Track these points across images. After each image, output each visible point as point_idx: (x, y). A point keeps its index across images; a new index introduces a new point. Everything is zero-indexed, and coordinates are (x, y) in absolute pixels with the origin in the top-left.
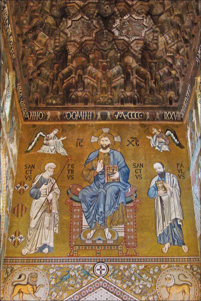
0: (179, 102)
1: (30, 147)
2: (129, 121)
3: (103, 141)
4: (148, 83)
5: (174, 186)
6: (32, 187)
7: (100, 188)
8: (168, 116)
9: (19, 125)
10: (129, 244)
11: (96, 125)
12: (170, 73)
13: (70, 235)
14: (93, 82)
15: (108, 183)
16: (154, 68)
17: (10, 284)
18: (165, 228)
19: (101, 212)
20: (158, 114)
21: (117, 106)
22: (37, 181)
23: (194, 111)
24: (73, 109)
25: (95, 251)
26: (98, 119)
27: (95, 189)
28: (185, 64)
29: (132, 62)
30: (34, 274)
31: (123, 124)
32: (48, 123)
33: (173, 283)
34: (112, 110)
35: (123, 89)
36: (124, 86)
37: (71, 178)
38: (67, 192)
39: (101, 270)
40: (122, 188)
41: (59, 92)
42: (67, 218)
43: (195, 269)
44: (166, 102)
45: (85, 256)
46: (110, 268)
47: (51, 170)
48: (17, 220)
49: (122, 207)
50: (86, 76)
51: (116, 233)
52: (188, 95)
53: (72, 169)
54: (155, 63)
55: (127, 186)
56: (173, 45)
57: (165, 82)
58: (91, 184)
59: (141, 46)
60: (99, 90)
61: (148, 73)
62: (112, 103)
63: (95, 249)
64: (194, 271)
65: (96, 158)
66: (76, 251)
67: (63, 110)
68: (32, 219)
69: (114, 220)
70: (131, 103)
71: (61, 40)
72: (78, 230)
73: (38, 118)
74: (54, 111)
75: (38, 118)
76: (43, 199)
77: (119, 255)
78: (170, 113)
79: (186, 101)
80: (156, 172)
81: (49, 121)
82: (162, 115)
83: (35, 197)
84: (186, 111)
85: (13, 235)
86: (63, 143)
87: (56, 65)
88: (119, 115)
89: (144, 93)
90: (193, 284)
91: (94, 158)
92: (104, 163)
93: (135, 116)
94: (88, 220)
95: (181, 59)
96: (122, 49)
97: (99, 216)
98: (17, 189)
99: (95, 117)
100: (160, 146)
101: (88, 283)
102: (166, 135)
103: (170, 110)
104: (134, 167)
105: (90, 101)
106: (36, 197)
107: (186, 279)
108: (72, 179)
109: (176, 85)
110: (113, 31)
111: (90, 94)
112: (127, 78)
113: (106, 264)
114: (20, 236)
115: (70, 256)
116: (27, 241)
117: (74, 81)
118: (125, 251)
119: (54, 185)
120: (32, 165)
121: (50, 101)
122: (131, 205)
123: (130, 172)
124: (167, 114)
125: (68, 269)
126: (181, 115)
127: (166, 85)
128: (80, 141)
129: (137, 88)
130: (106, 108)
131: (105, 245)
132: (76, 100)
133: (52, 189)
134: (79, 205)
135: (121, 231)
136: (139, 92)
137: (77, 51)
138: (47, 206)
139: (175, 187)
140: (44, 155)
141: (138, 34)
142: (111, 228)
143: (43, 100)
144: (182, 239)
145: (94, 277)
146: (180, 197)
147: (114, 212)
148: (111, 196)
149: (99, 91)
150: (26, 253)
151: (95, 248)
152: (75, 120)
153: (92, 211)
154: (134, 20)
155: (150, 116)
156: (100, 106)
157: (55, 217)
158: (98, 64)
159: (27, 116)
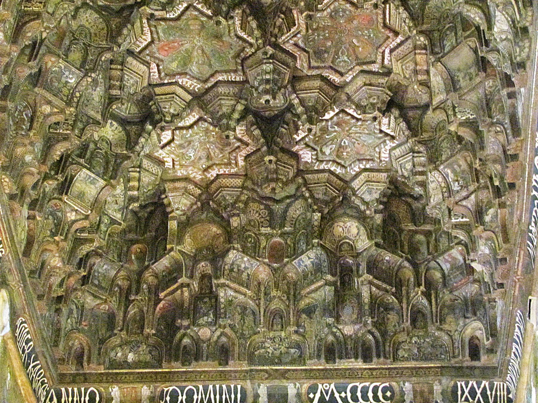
0: (498, 353)
16: (423, 249)
20: (437, 388)
21: (314, 367)
24: (188, 377)
29: (358, 234)
34: (300, 379)
41: (146, 326)
44: (459, 355)
50: (222, 281)
54: (428, 234)
56: (466, 198)
57: (456, 293)
59: (382, 188)
60: (262, 318)
61: (406, 264)
62: (301, 359)
70: (356, 358)
71: (146, 179)
74: (131, 385)
78: (475, 386)
82: (449, 390)
87: (136, 248)
88: (321, 392)
89: (395, 326)
96: (326, 198)
105: (236, 356)
110: (294, 149)
111: (236, 333)
117: (186, 294)
124: (467, 387)
126: (509, 392)
127: (459, 301)
129: (372, 314)
130: (284, 375)
136: (380, 325)
137: (195, 207)
141: (370, 156)
143: (97, 352)
149: (262, 321)
154: (354, 121)
155: (414, 394)
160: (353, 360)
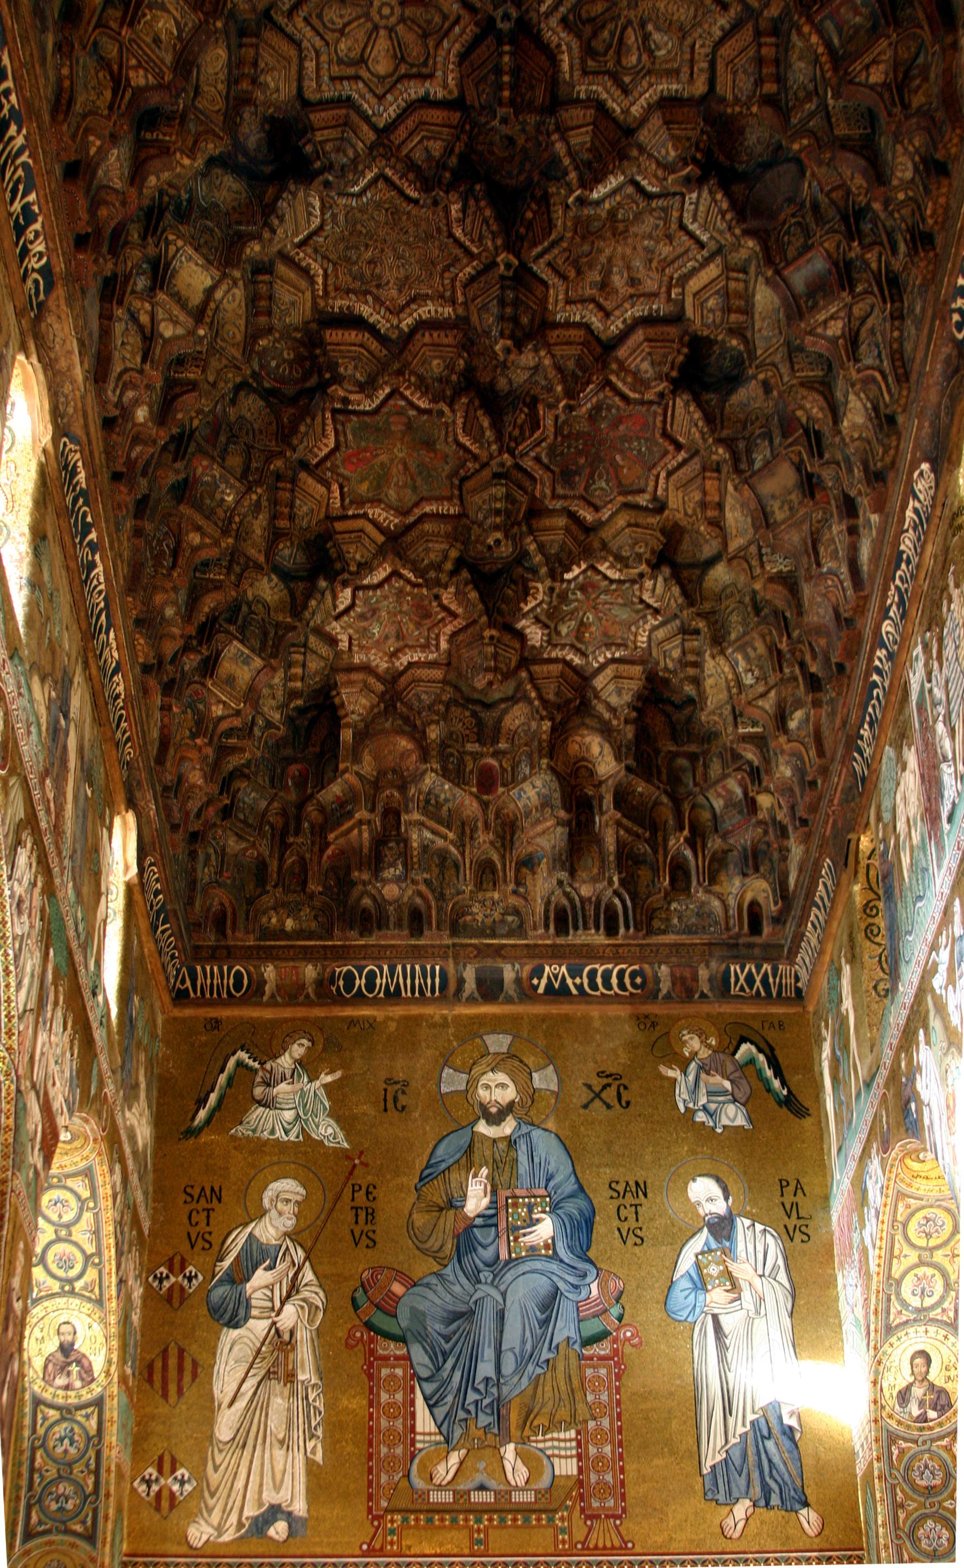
1: (202, 1114)
2: (590, 1003)
3: (488, 1087)
4: (666, 841)
6: (214, 1276)
7: (479, 1282)
8: (746, 979)
9: (154, 1021)
11: (457, 1018)
12: (752, 805)
13: (370, 1471)
14: (445, 841)
15: (510, 1260)
18: (733, 1441)
19: (487, 1380)
20: (703, 973)
23: (847, 969)
25: (465, 1532)
26: (465, 995)
27: (460, 1285)
28: (808, 778)
31: (566, 1015)
32: (268, 1014)
35: (563, 869)
38: (354, 1300)
42: (356, 1403)
45: (427, 1552)
47: (289, 1209)
48: (163, 1409)
49: (567, 1358)
51: (545, 1461)
53: (368, 1204)
62: (520, 931)
63: (467, 1527)
66: (392, 1532)
67: (325, 959)
72: (399, 1451)
76: (258, 1327)
77: (556, 1546)
80: (698, 1215)
83: (227, 1316)
84: (816, 962)
85: (150, 1470)
86: (329, 1098)
91: (451, 1161)
92: (491, 1178)
93: (614, 981)
94: (436, 1410)
95: (793, 754)
97: (477, 1397)
98: (156, 1284)
99: (452, 987)
100: (712, 1106)
102: (735, 1062)
103: (750, 958)
109: (776, 855)
112: (579, 824)
114: (178, 1473)
115: (370, 1552)
116: (206, 1494)
118: (579, 1535)
120: (212, 1189)
126: (797, 979)
130: (498, 951)
134: (402, 1352)
139: (774, 1276)
142: (524, 1441)
144: (799, 1483)
146: (791, 1315)
147: (536, 1382)
150: (205, 1538)
151: (466, 1520)
152: (375, 1001)
153: (451, 1376)
158: (461, 763)
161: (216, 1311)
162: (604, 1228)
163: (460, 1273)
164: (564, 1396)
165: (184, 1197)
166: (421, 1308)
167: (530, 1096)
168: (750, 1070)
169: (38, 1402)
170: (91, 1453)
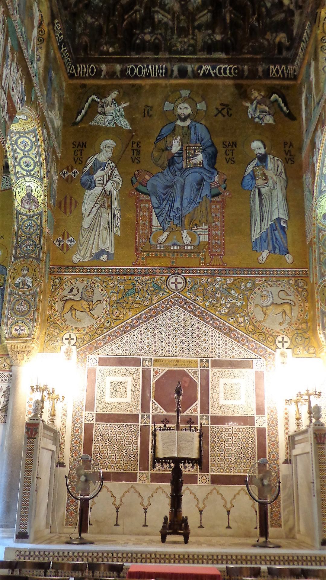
1: (79, 117)
3: (181, 108)
5: (278, 174)
7: (176, 175)
9: (61, 85)
10: (214, 251)
11: (171, 85)
13: (136, 238)
15: (187, 168)
17: (59, 299)
18: (264, 231)
20: (260, 69)
22: (90, 165)
23: (313, 63)
27: (169, 176)
30: (89, 288)
32: (103, 82)
33: (270, 302)
36: (211, 26)
37: (136, 161)
38: (132, 181)
39: (176, 283)
40: (206, 176)
42: (131, 215)
43: (300, 285)
46: (188, 281)
49: (206, 202)
50: (157, 9)
52: (305, 38)
53: (138, 148)
55: (213, 174)
57: (273, 19)
58: (164, 170)
62: (194, 53)
64: (299, 287)
65: (172, 134)
66: (143, 259)
68: (84, 216)
69: (194, 219)
70: (222, 52)
72: (146, 232)
73: (89, 74)
75: (89, 74)
76: (98, 190)
77: (200, 264)
78: (279, 68)
79: (303, 49)
81: (105, 78)
84: (302, 63)
85: (60, 237)
90: (296, 303)
91: (167, 134)
92: (181, 140)
93: (228, 71)
94: (159, 218)
100: (261, 116)
101: (159, 300)
104: (224, 147)
106: (89, 187)
107: (288, 298)
108: (138, 162)
113: (183, 276)
114: (70, 239)
116: (79, 246)
117: (138, 16)
118: (208, 260)
119: (113, 170)
120: (83, 143)
121: (105, 48)
122: (218, 199)
123: (218, 154)
125: (133, 281)
128: (148, 108)
130: (186, 60)
131: (182, 251)
132: (143, 47)
133: (111, 176)
135: (203, 233)
138: (104, 199)
139: (280, 175)
140: (99, 128)
142: (190, 229)
144: (286, 246)
145: (167, 292)
146: (286, 188)
147: (195, 209)
148: (191, 186)
150: (79, 260)
151: (169, 255)
152: (142, 78)
153: (165, 207)
156: (177, 56)
157: (115, 214)
159: (72, 70)
160: (220, 53)
161: (83, 185)
162: (221, 157)
163: (170, 173)
164: (204, 214)
165: (73, 146)
166: (155, 184)
167: (196, 112)
168: (275, 103)
169: (19, 214)
170: (38, 231)
